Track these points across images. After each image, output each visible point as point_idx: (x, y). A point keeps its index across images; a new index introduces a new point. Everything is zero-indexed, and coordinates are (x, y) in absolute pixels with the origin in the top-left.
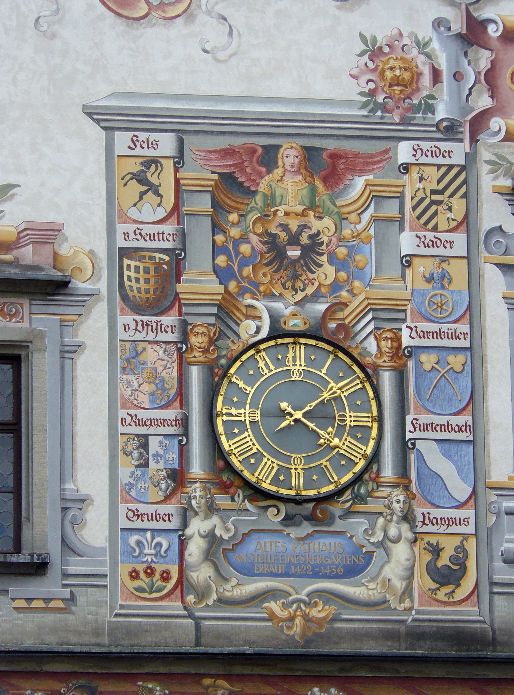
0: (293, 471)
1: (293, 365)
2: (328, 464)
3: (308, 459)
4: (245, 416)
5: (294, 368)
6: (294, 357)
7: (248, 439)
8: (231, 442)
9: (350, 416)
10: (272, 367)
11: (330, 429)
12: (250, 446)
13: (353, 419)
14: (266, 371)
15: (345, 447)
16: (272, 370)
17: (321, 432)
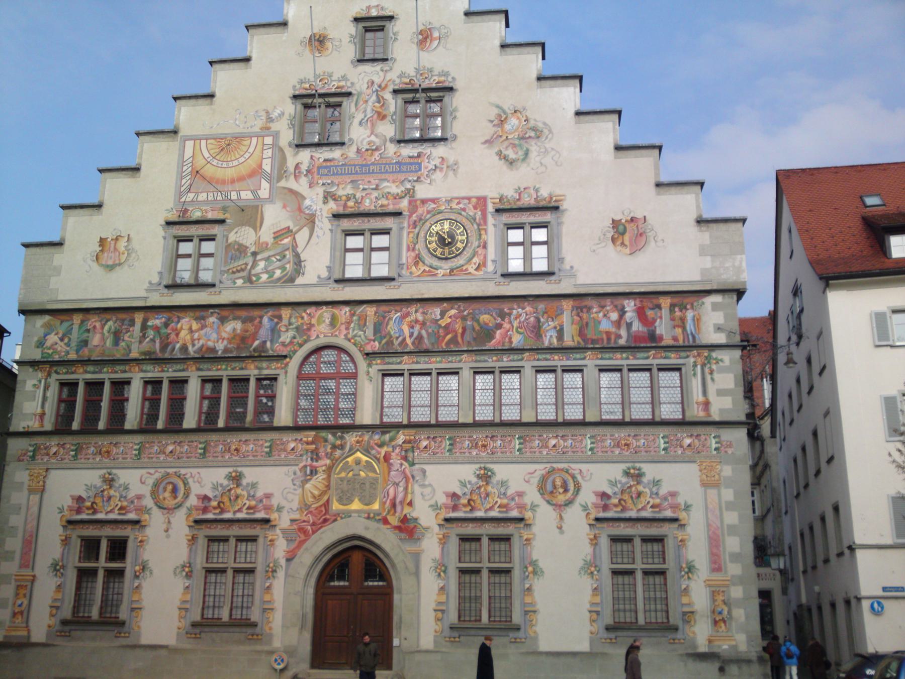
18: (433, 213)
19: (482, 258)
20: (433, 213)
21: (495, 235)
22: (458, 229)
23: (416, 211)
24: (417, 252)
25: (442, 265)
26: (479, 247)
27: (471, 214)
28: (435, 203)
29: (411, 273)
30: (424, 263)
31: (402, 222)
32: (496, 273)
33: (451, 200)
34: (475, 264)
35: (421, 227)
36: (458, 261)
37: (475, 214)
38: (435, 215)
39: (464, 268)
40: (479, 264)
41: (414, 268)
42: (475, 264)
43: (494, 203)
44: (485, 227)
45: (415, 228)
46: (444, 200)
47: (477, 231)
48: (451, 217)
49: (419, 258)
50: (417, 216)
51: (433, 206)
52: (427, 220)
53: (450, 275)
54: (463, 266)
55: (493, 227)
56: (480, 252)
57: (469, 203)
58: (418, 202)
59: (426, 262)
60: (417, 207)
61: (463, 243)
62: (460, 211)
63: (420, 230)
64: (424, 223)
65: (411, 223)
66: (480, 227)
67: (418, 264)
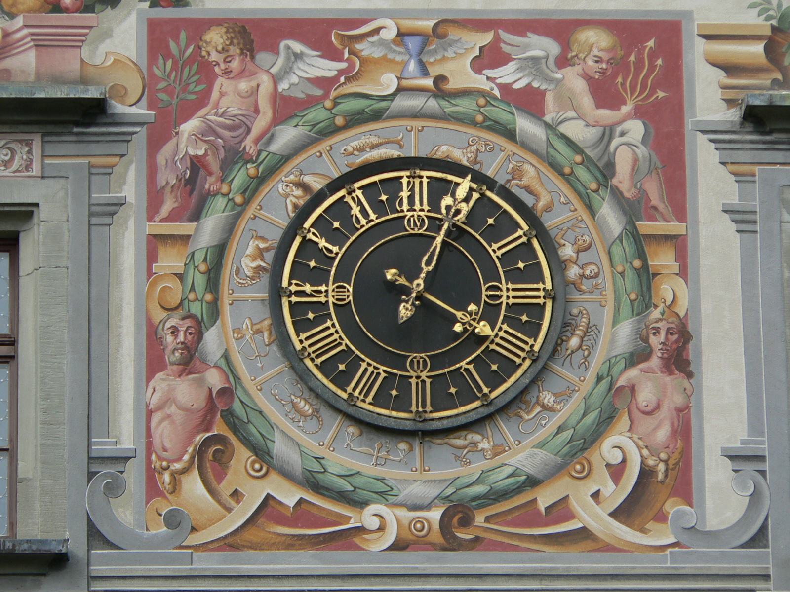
0: (413, 381)
1: (408, 210)
2: (471, 367)
3: (437, 362)
4: (326, 296)
5: (410, 214)
6: (411, 199)
7: (332, 330)
8: (303, 336)
9: (508, 289)
10: (373, 216)
11: (472, 307)
12: (336, 340)
13: (511, 294)
14: (363, 221)
15: (498, 340)
16: (372, 220)
17: (459, 314)
18: (317, 114)
19: (663, 434)
20: (317, 114)
21: (748, 283)
22: (493, 234)
23: (203, 100)
24: (214, 379)
25: (391, 473)
26: (638, 356)
27: (575, 130)
28: (333, 55)
29: (173, 520)
30: (262, 453)
31: (107, 171)
32: (759, 539)
33: (439, 32)
34: (617, 472)
35: (238, 212)
36: (497, 451)
37: (608, 133)
38: (332, 130)
39: (544, 498)
40: (646, 474)
41: (193, 485)
42: (617, 472)
43: (730, 69)
44: (675, 227)
45: (196, 216)
46: (390, 33)
47: (629, 246)
48: (443, 151)
49: (230, 418)
50: (209, 130)
51: (327, 68)
52: (285, 159)
53: (451, 544)
54: (532, 482)
55: (727, 226)
56: (645, 396)
57: (563, 62)
58: (215, 37)
59: (279, 447)
60: (207, 72)
61: (533, 329)
62: (500, 113)
63: (230, 229)
64: (261, 180)
65: (167, 177)
66: (645, 227)
67: (222, 460)
